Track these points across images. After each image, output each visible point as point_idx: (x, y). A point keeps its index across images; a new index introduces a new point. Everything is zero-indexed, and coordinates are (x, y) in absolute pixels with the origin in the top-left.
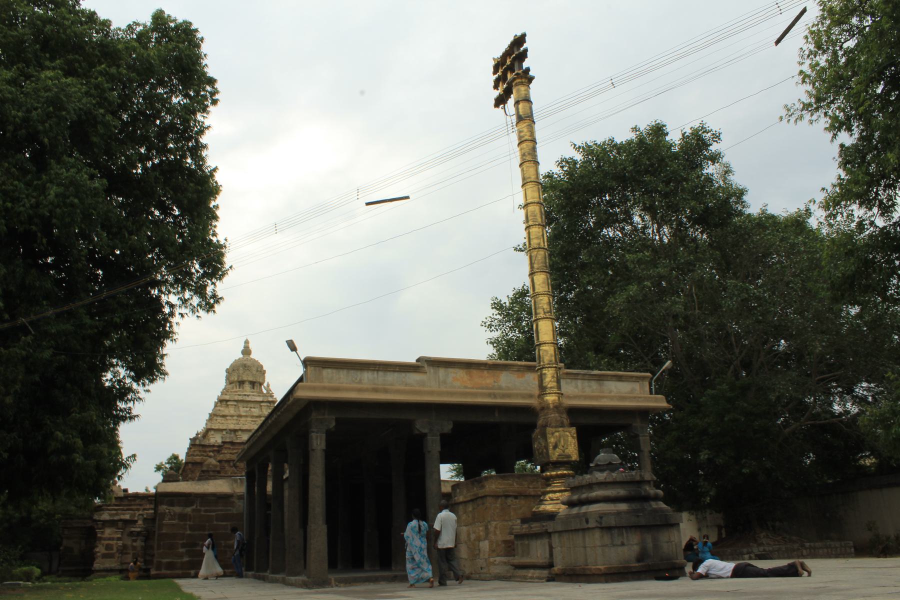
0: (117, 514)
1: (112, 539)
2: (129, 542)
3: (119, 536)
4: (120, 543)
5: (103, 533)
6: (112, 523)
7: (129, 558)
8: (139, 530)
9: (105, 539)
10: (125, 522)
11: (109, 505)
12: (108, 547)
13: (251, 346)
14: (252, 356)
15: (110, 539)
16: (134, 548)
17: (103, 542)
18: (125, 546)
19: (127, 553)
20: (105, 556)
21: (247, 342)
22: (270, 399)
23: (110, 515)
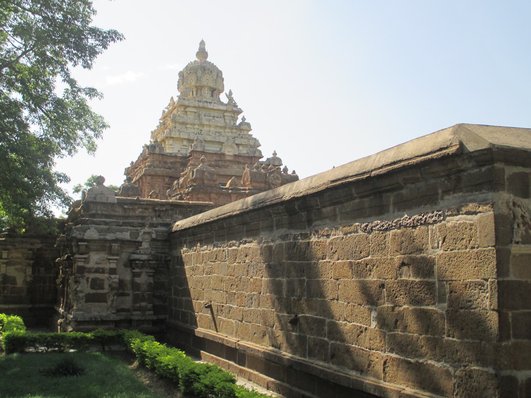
0: (109, 231)
1: (103, 271)
2: (128, 277)
3: (113, 266)
4: (115, 278)
5: (87, 260)
6: (104, 245)
7: (128, 302)
8: (145, 257)
9: (90, 271)
10: (123, 242)
11: (94, 216)
12: (96, 284)
13: (207, 49)
14: (208, 60)
15: (97, 271)
16: (135, 286)
17: (87, 275)
18: (121, 282)
19: (123, 295)
20: (90, 298)
21: (202, 43)
22: (235, 109)
23: (100, 231)
